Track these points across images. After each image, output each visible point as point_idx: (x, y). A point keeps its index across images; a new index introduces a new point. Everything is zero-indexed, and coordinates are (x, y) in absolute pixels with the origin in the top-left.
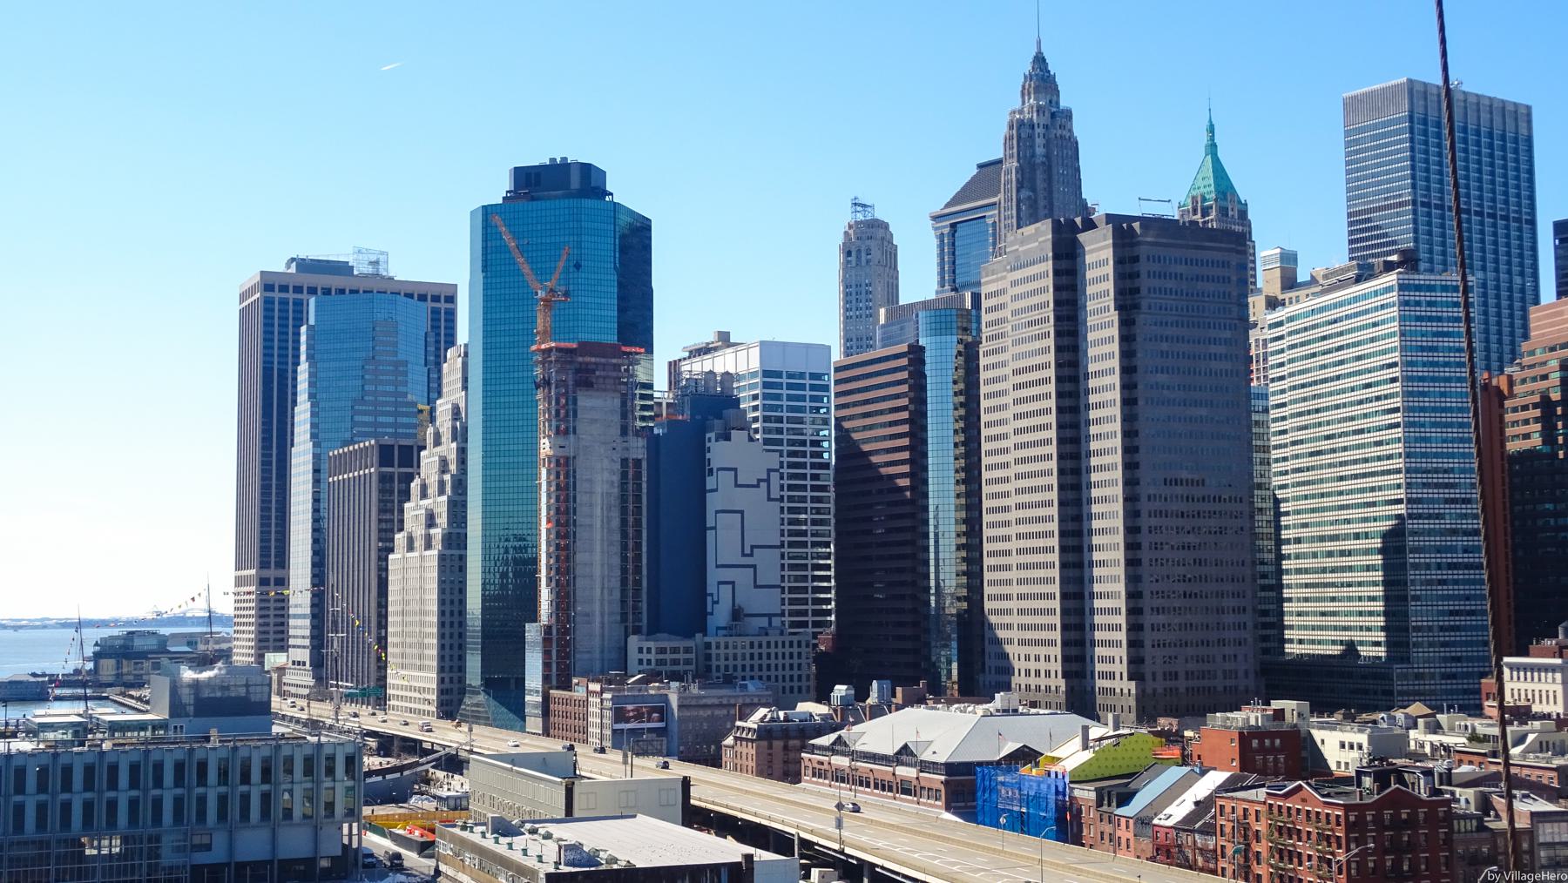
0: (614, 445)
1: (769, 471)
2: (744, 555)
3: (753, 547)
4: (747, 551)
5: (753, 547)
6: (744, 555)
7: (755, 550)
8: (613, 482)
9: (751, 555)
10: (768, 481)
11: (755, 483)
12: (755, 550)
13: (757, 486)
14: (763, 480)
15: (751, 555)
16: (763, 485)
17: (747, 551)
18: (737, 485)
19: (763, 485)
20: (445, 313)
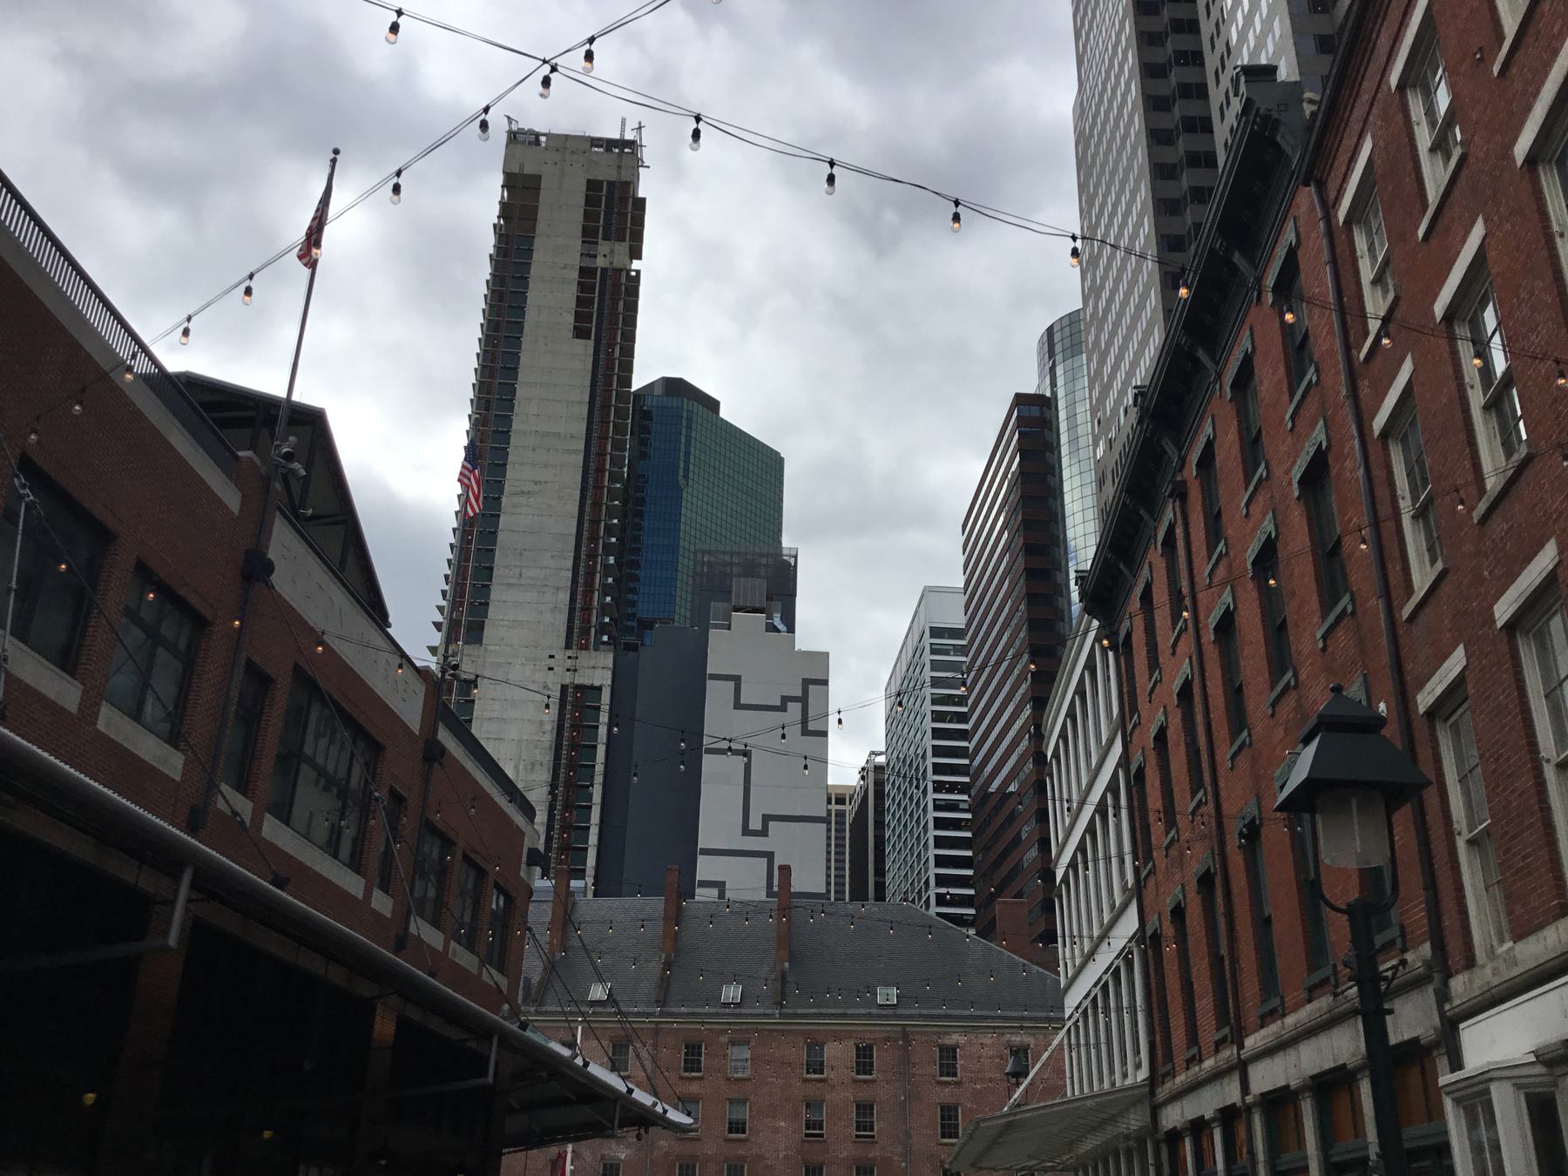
0: (551, 662)
1: (807, 683)
2: (746, 831)
3: (767, 819)
4: (756, 824)
5: (767, 819)
6: (746, 831)
7: (771, 824)
8: (542, 723)
9: (764, 832)
10: (803, 700)
11: (778, 703)
12: (771, 824)
13: (782, 708)
14: (794, 699)
15: (764, 832)
16: (794, 709)
17: (756, 824)
18: (738, 705)
19: (794, 709)
20: (836, 815)
